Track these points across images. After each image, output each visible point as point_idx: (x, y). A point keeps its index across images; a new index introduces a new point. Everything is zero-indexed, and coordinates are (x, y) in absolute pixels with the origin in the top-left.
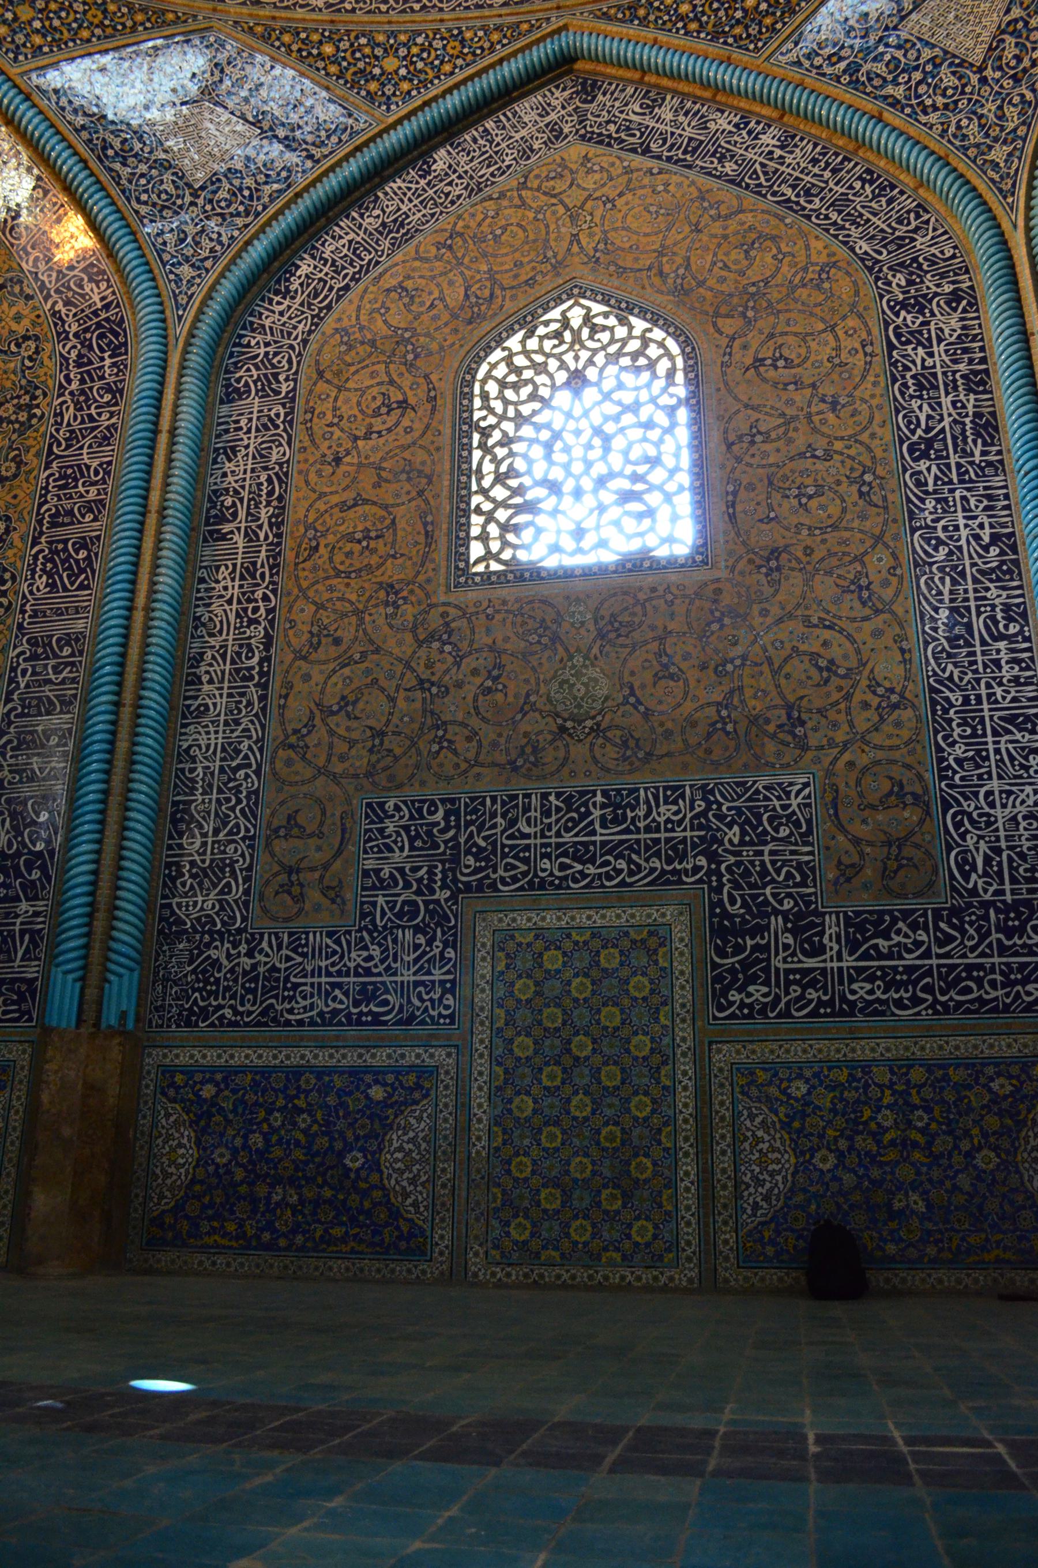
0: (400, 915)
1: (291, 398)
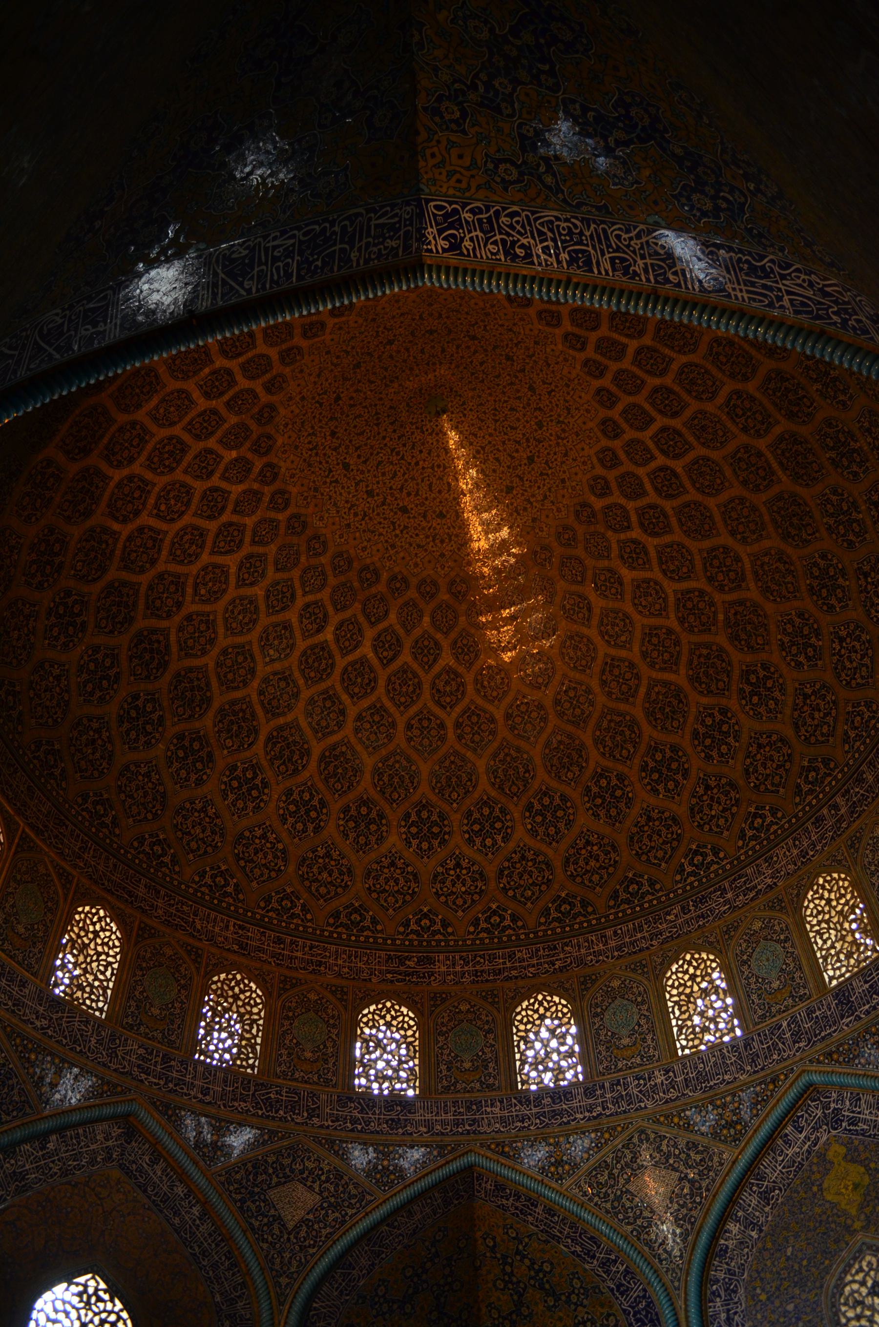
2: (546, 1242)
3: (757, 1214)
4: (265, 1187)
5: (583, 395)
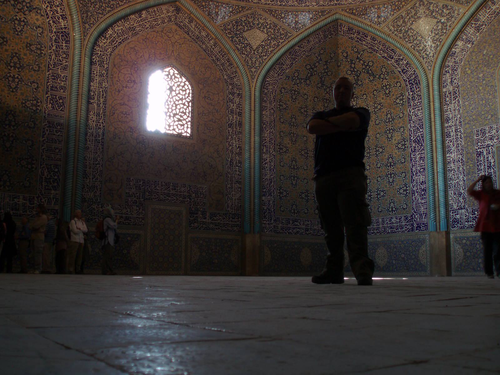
0: (133, 203)
1: (107, 70)
2: (371, 53)
3: (472, 37)
4: (242, 31)
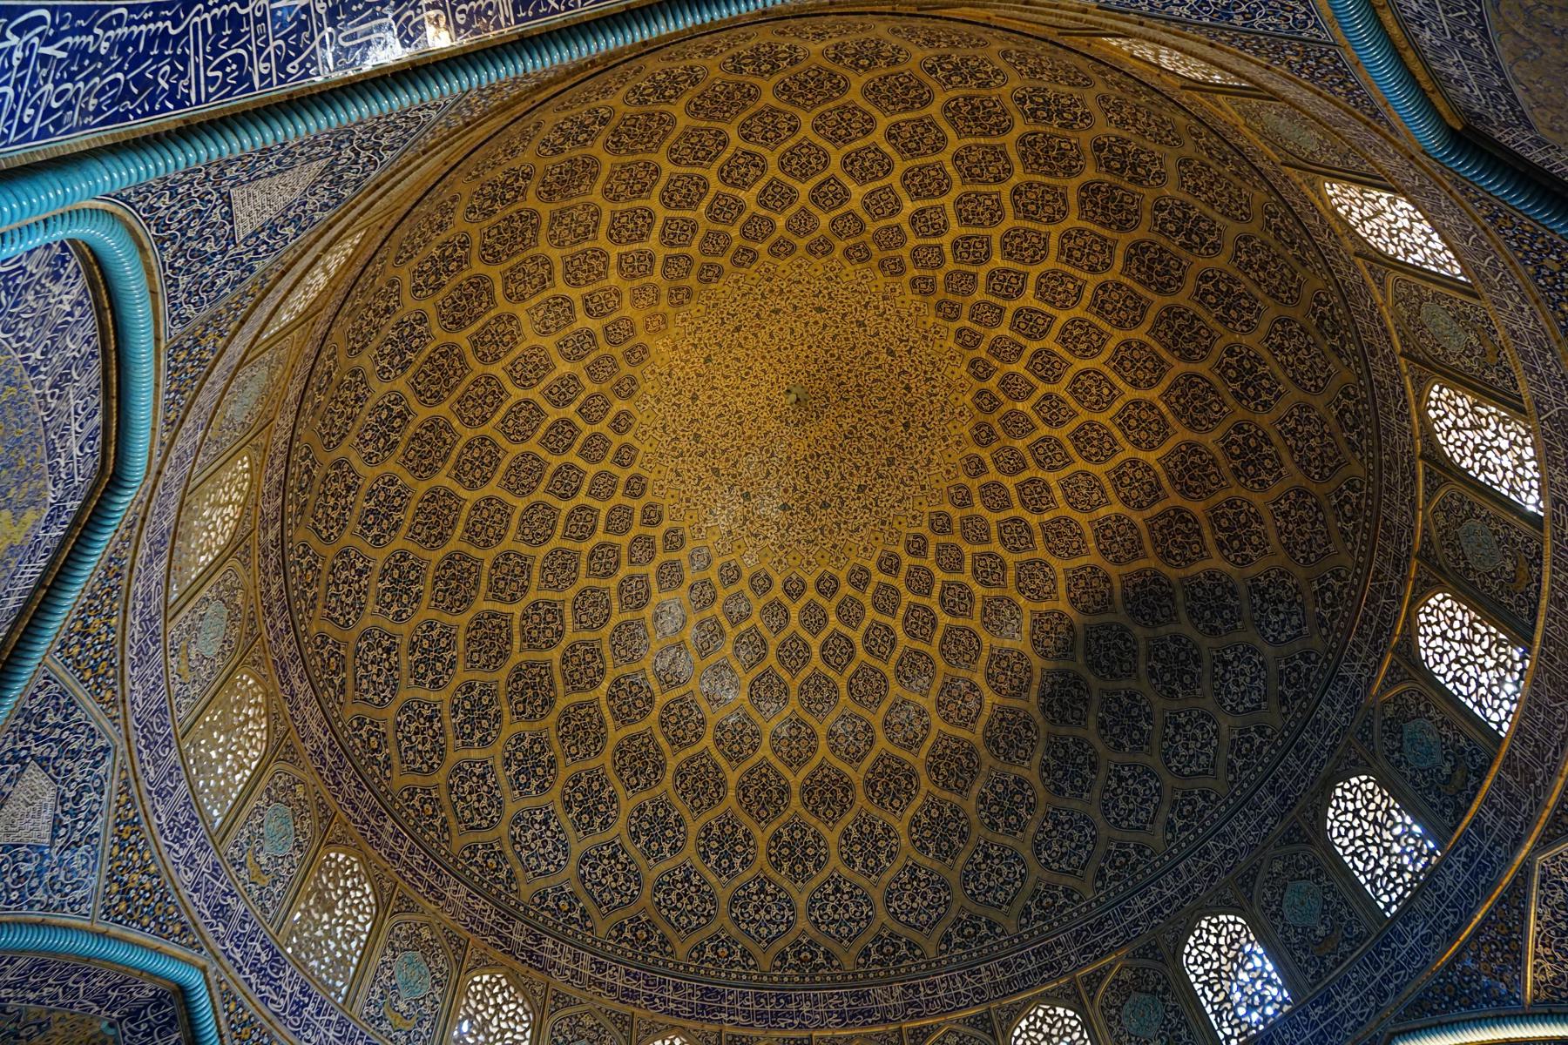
5: (672, 501)
